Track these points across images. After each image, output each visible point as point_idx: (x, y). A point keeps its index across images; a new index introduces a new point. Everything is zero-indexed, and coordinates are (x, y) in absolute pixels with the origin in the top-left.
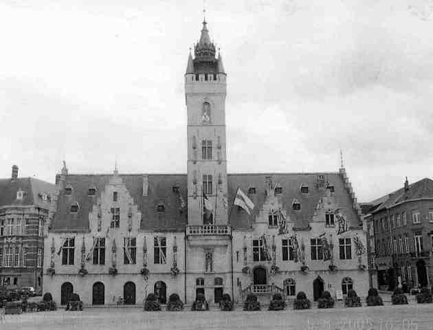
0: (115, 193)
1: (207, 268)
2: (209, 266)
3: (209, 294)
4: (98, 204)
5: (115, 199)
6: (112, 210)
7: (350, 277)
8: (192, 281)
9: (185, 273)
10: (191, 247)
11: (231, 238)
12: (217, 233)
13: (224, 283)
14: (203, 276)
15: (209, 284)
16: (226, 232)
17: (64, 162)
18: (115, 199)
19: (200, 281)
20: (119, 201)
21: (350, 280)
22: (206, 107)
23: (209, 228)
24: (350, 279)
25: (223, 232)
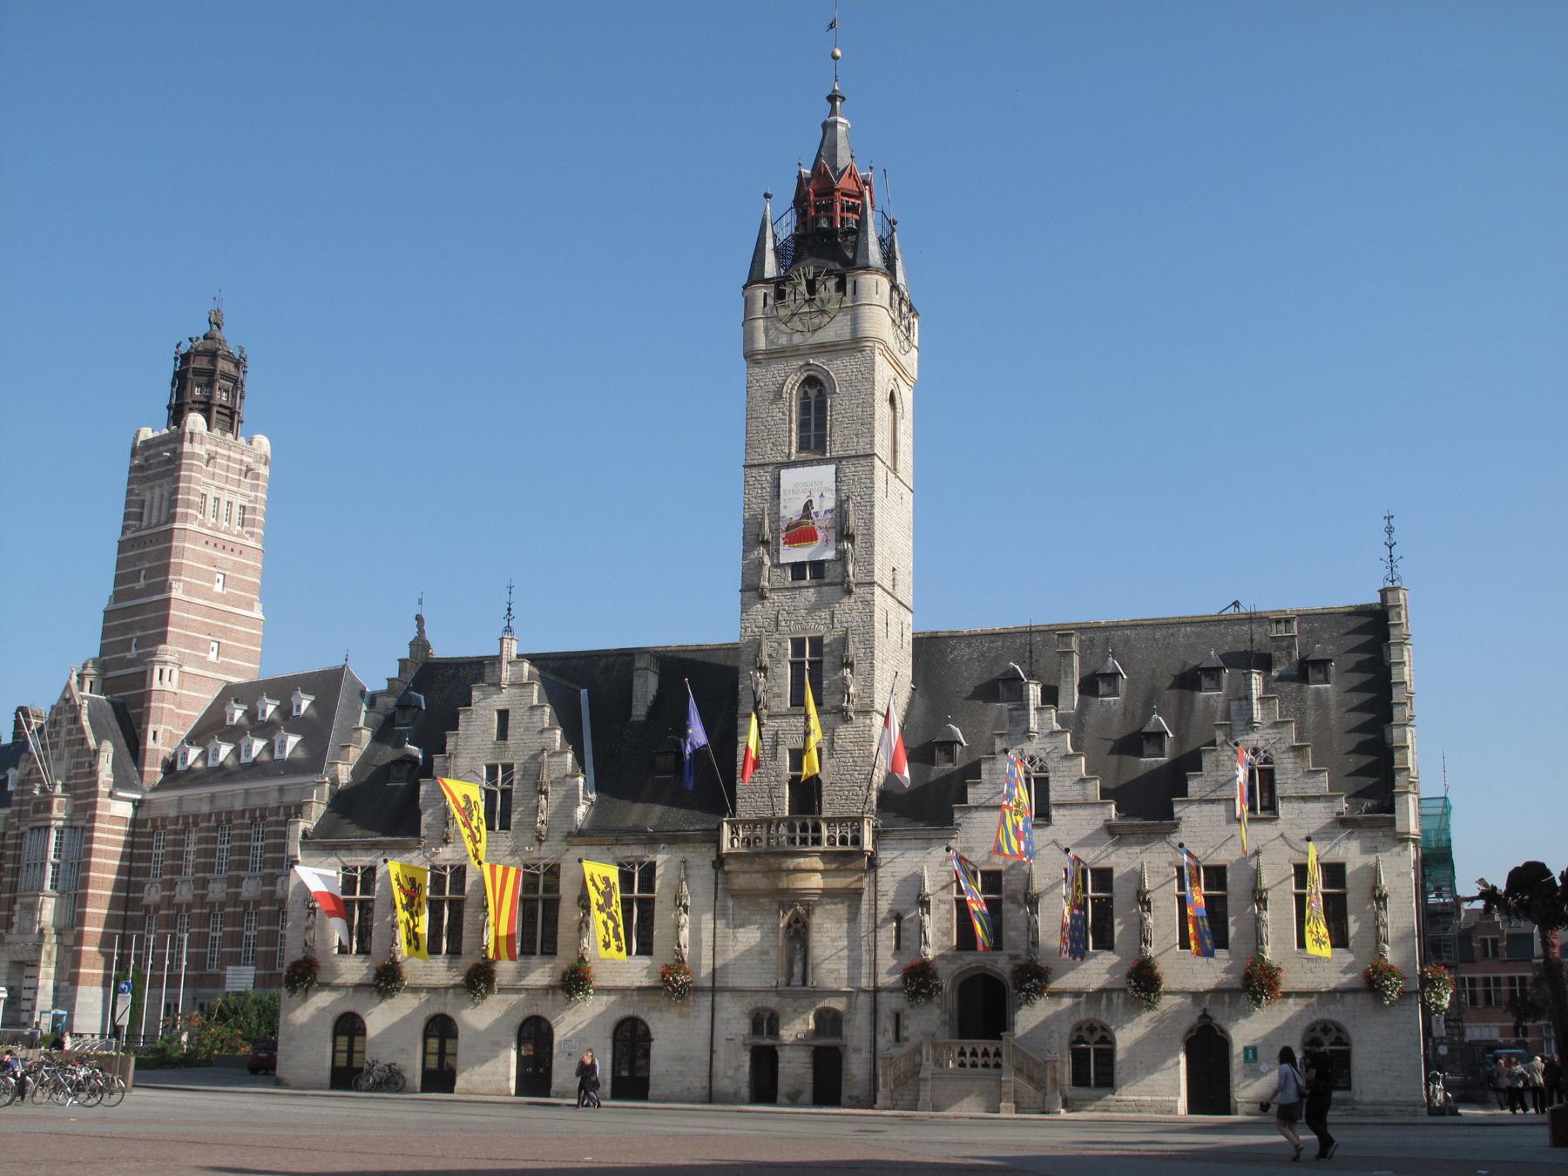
0: (503, 715)
1: (790, 975)
2: (797, 969)
3: (794, 1067)
4: (449, 747)
5: (503, 733)
6: (492, 770)
7: (1333, 1017)
8: (734, 1021)
9: (713, 990)
10: (736, 895)
11: (873, 864)
12: (825, 846)
13: (845, 1031)
14: (772, 1002)
15: (797, 1027)
16: (857, 841)
17: (419, 619)
18: (503, 733)
19: (765, 1023)
20: (511, 741)
21: (1342, 1038)
22: (813, 393)
23: (804, 828)
24: (1339, 1029)
25: (843, 841)
